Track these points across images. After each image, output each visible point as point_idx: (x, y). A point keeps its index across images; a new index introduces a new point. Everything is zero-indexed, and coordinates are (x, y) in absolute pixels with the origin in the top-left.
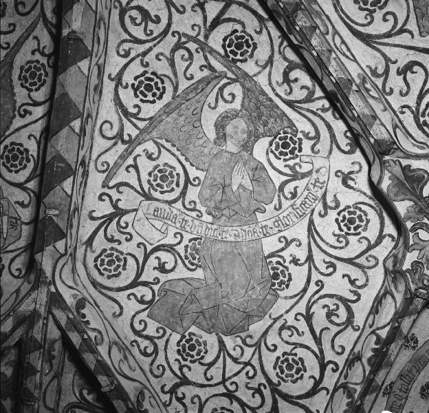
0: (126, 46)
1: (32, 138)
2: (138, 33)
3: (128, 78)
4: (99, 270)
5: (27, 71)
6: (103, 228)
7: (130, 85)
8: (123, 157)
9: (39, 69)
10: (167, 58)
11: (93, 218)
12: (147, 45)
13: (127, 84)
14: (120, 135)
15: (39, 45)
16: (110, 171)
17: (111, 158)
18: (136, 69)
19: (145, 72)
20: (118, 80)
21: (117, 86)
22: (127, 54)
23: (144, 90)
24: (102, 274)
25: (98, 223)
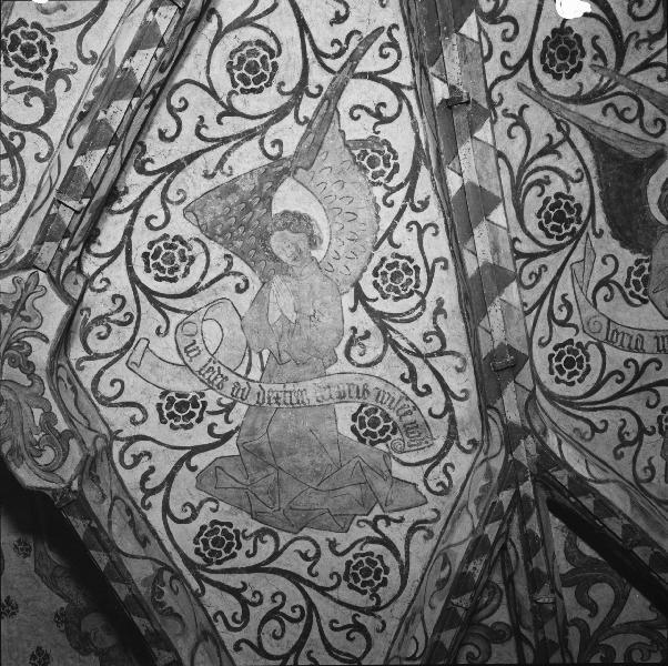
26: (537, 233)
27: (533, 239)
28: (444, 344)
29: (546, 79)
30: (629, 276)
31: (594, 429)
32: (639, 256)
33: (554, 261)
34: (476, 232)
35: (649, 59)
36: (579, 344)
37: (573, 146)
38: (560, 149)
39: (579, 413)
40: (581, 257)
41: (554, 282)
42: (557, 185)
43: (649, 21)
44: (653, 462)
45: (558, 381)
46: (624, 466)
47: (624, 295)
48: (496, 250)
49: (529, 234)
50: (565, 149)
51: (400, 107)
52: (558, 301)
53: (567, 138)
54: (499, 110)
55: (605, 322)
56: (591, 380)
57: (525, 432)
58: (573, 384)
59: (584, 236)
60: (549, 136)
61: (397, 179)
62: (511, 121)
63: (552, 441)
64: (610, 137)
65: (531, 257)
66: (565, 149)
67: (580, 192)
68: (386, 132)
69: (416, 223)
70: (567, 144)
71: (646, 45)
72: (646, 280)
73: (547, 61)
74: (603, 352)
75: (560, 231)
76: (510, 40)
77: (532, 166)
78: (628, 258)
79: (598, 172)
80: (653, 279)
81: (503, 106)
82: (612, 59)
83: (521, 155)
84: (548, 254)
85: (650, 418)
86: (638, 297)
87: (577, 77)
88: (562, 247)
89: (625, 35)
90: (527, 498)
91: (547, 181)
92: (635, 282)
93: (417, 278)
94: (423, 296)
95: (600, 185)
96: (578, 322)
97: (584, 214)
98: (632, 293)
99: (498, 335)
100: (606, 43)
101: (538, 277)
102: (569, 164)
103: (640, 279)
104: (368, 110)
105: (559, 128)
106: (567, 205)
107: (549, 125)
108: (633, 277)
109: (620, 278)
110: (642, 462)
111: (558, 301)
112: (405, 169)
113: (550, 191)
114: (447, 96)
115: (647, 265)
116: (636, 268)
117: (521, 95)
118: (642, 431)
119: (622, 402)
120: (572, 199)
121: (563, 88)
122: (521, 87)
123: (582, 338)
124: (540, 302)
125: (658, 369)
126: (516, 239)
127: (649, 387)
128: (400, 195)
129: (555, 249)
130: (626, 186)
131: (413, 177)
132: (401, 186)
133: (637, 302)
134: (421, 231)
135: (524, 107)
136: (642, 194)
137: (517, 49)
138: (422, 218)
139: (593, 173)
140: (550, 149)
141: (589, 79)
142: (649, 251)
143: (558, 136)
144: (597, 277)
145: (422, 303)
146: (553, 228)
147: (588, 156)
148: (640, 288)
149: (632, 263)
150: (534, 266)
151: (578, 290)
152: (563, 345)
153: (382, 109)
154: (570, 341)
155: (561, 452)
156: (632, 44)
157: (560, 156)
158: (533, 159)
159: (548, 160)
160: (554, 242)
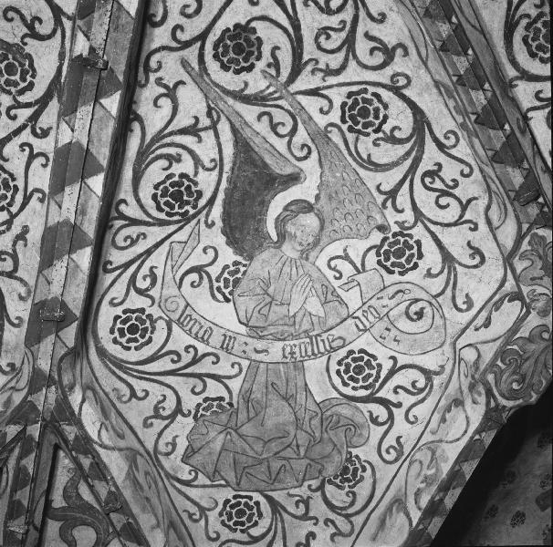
26: (149, 204)
27: (142, 207)
28: (16, 269)
29: (213, 66)
30: (222, 273)
31: (133, 394)
32: (239, 259)
33: (156, 233)
34: (67, 189)
35: (318, 89)
36: (149, 316)
37: (217, 136)
38: (202, 134)
39: (124, 376)
40: (184, 239)
41: (149, 252)
42: (186, 166)
43: (330, 56)
44: (178, 440)
45: (115, 341)
46: (149, 437)
47: (211, 287)
48: (81, 211)
49: (138, 201)
50: (208, 137)
51: (54, 31)
52: (145, 270)
53: (214, 127)
54: (152, 77)
55: (182, 304)
56: (147, 352)
57: (49, 381)
58: (129, 349)
59: (195, 221)
60: (197, 119)
61: (27, 97)
62: (163, 91)
63: (76, 398)
64: (256, 143)
65: (134, 222)
66: (208, 137)
67: (206, 181)
68: (32, 46)
69: (30, 146)
70: (211, 132)
71: (322, 74)
72: (237, 282)
73: (221, 50)
74: (170, 330)
75: (172, 207)
76: (189, 16)
77: (167, 140)
78: (228, 256)
79: (233, 169)
80: (244, 284)
81: (158, 74)
82: (285, 72)
83: (159, 125)
84: (153, 225)
85: (190, 402)
86: (224, 295)
87: (244, 76)
88: (169, 223)
89: (306, 57)
90: (31, 438)
91: (178, 159)
92: (226, 280)
93: (13, 197)
94: (13, 216)
95: (229, 180)
96: (156, 296)
97: (202, 202)
98: (219, 289)
99: (56, 289)
100: (286, 58)
101: (134, 242)
102: (206, 150)
103: (231, 279)
104: (23, 18)
105: (209, 114)
106: (188, 188)
107: (201, 109)
108: (226, 275)
109: (214, 271)
110: (167, 437)
111: (145, 270)
112: (39, 91)
113: (177, 169)
114: (85, 54)
115: (242, 269)
116: (232, 268)
117: (182, 70)
118: (179, 410)
119: (169, 380)
120: (196, 184)
121: (229, 80)
122: (185, 64)
123: (155, 311)
124: (127, 265)
125: (213, 363)
126: (124, 201)
127: (199, 376)
128: (24, 114)
129: (161, 223)
130: (253, 191)
131: (43, 103)
132: (28, 105)
133: (220, 297)
134: (32, 157)
135: (181, 83)
136: (265, 205)
137: (194, 28)
138: (39, 145)
139: (227, 167)
140: (193, 130)
141: (256, 82)
142: (251, 258)
143: (205, 122)
144: (192, 262)
145: (9, 223)
146: (167, 203)
147: (229, 150)
148: (227, 287)
149: (230, 262)
150: (133, 231)
151: (169, 267)
152: (133, 311)
153: (37, 25)
154: (142, 311)
155: (80, 409)
156: (309, 68)
157: (200, 140)
158: (171, 134)
159: (188, 140)
160: (162, 216)
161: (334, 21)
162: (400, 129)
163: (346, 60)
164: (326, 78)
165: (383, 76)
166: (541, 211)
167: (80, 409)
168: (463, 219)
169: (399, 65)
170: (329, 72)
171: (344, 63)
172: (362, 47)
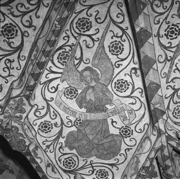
0: (157, 19)
1: (126, 75)
2: (161, 10)
3: (162, 32)
4: (175, 117)
5: (112, 47)
6: (172, 100)
7: (164, 35)
8: (171, 67)
9: (118, 44)
10: (177, 16)
11: (166, 98)
12: (166, 14)
13: (162, 35)
14: (166, 58)
15: (114, 33)
16: (167, 76)
17: (166, 70)
18: (165, 26)
19: (169, 26)
20: (158, 35)
21: (158, 38)
22: (159, 22)
23: (171, 34)
24: (177, 118)
25: (169, 99)
35: (5, 14)
43: (17, 11)
71: (10, 12)
89: (11, 5)
156: (9, 8)
161: (27, 5)
162: (14, 44)
163: (19, 16)
164: (10, 14)
165: (24, 29)
166: (29, 95)
167: (69, 175)
168: (6, 78)
169: (30, 31)
170: (12, 14)
171: (18, 16)
172: (27, 17)
